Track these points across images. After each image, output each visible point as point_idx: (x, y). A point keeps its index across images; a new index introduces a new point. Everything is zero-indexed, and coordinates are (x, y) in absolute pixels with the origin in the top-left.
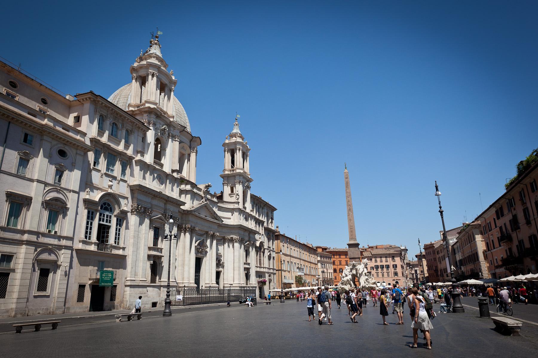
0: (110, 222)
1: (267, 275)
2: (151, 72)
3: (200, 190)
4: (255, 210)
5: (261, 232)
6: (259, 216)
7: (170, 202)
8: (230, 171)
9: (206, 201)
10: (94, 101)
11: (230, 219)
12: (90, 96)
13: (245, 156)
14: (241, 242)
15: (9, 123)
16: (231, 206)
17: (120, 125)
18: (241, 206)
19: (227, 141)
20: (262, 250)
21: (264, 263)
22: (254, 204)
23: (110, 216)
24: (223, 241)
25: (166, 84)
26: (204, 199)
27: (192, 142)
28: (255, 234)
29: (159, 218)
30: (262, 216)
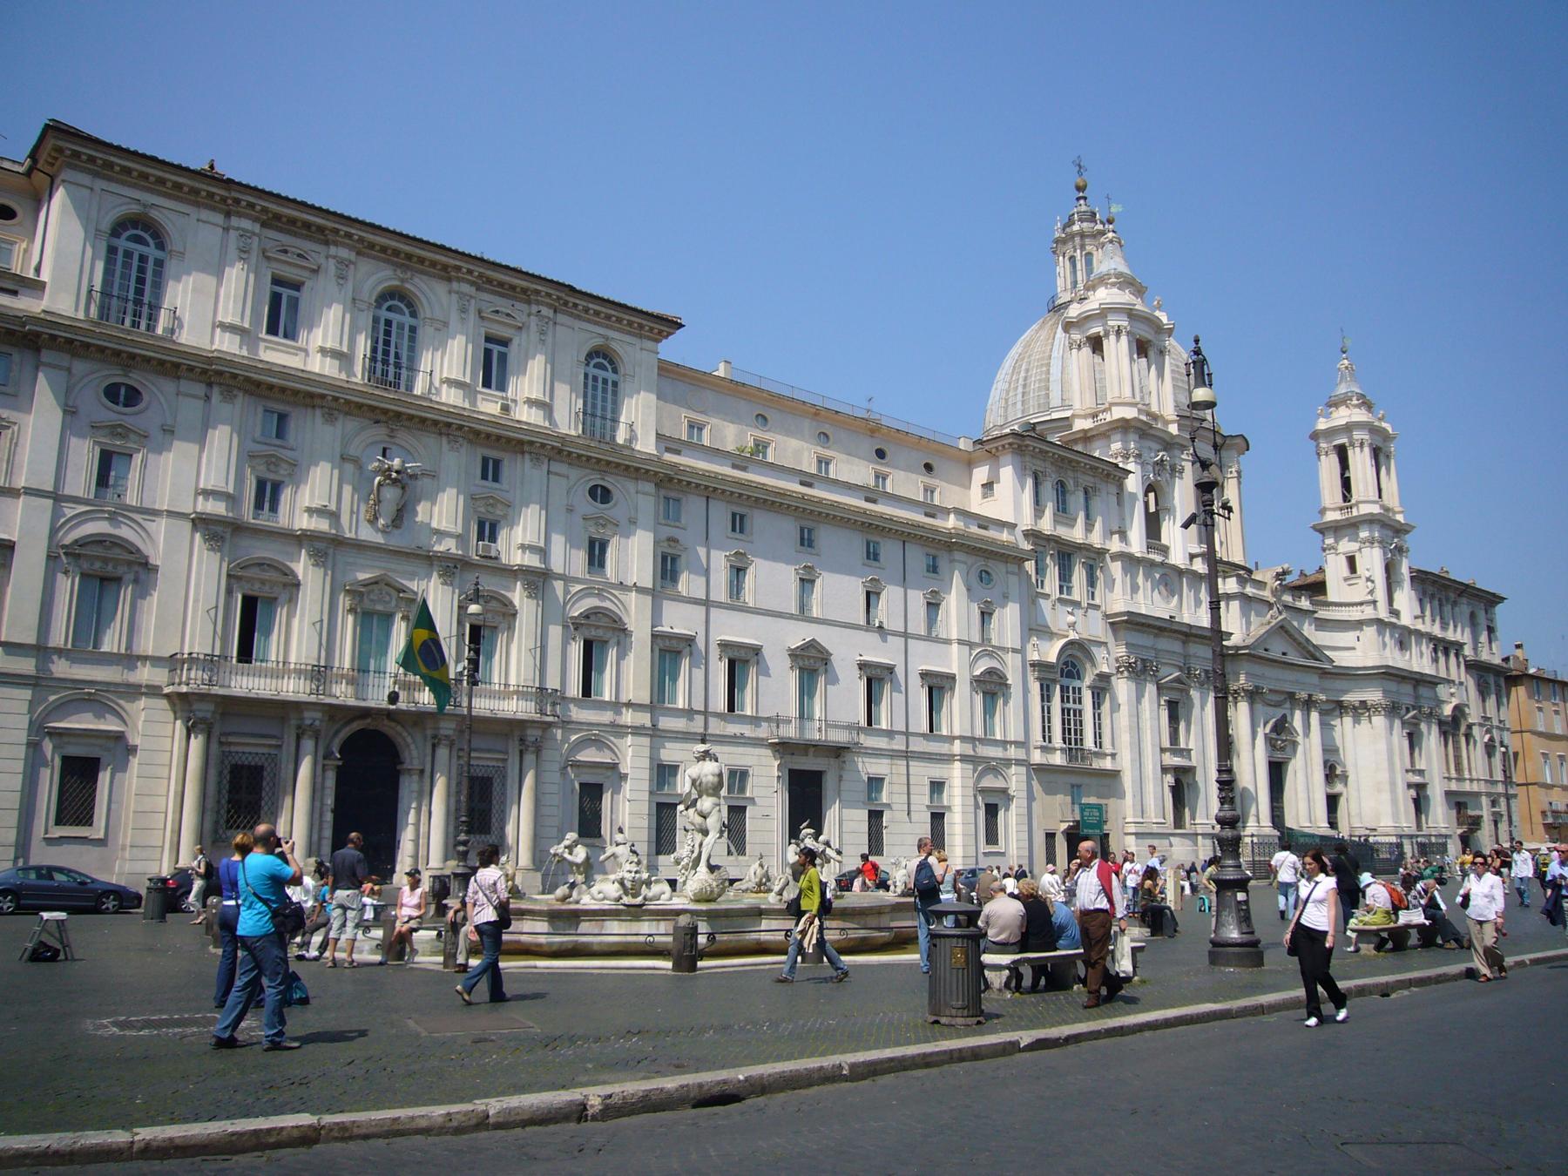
0: (1080, 703)
1: (1485, 801)
2: (1113, 327)
3: (1261, 584)
4: (1428, 613)
5: (1454, 675)
6: (1444, 626)
7: (1196, 636)
8: (1341, 509)
9: (1280, 613)
10: (1019, 446)
11: (1354, 649)
12: (1011, 440)
13: (1382, 458)
14: (1392, 710)
15: (904, 542)
16: (1354, 614)
17: (1072, 482)
18: (1383, 613)
19: (1322, 425)
20: (1463, 729)
21: (1473, 765)
22: (1424, 593)
23: (1080, 689)
24: (1337, 713)
25: (1150, 341)
26: (1275, 609)
27: (1224, 453)
28: (1437, 684)
29: (1177, 680)
30: (1455, 627)
